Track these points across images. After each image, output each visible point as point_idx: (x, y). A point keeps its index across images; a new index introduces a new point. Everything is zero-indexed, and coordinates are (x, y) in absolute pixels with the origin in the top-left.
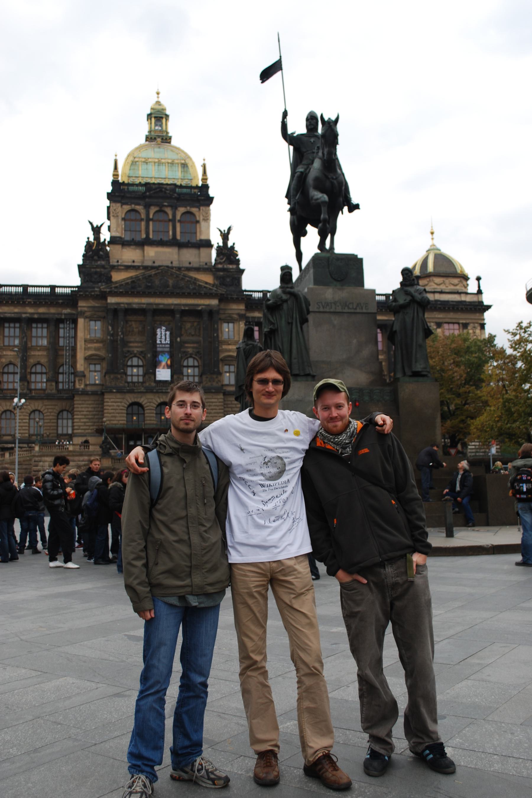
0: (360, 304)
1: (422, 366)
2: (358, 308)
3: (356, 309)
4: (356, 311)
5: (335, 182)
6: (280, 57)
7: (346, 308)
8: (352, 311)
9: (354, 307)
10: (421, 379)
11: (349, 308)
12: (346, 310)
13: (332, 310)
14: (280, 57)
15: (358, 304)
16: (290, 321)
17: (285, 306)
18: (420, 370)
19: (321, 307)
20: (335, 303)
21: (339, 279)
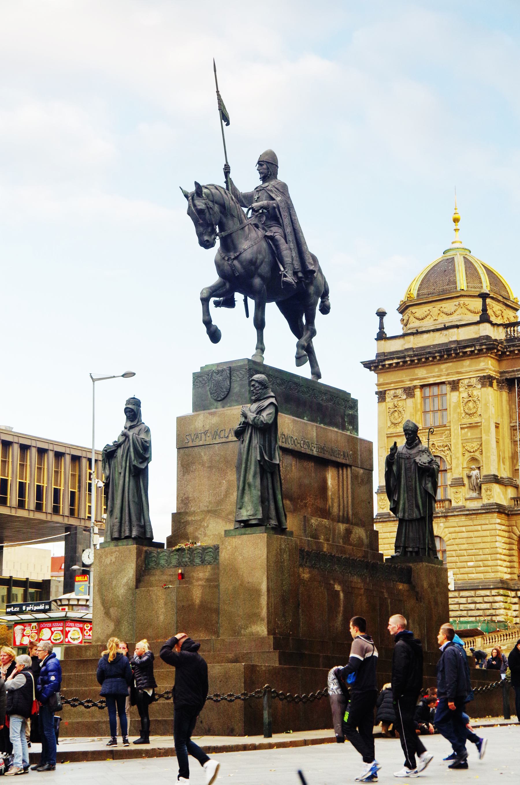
0: (233, 429)
1: (249, 513)
2: (230, 435)
3: (228, 437)
4: (227, 440)
5: (236, 262)
6: (218, 92)
7: (217, 437)
8: (224, 440)
9: (226, 436)
10: (249, 530)
11: (220, 437)
12: (218, 441)
13: (201, 443)
14: (218, 92)
15: (230, 431)
16: (120, 471)
17: (120, 452)
18: (245, 518)
19: (191, 442)
20: (206, 433)
21: (219, 399)
